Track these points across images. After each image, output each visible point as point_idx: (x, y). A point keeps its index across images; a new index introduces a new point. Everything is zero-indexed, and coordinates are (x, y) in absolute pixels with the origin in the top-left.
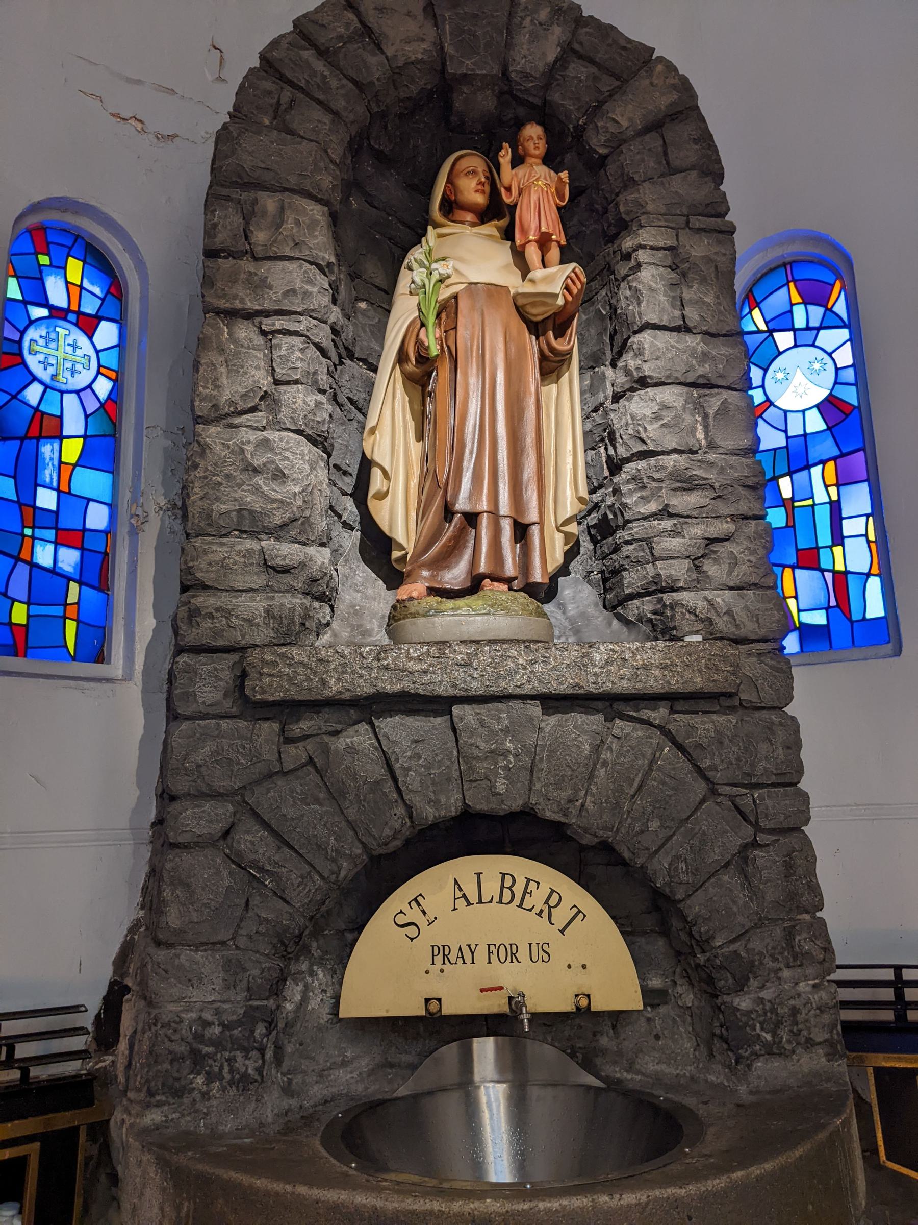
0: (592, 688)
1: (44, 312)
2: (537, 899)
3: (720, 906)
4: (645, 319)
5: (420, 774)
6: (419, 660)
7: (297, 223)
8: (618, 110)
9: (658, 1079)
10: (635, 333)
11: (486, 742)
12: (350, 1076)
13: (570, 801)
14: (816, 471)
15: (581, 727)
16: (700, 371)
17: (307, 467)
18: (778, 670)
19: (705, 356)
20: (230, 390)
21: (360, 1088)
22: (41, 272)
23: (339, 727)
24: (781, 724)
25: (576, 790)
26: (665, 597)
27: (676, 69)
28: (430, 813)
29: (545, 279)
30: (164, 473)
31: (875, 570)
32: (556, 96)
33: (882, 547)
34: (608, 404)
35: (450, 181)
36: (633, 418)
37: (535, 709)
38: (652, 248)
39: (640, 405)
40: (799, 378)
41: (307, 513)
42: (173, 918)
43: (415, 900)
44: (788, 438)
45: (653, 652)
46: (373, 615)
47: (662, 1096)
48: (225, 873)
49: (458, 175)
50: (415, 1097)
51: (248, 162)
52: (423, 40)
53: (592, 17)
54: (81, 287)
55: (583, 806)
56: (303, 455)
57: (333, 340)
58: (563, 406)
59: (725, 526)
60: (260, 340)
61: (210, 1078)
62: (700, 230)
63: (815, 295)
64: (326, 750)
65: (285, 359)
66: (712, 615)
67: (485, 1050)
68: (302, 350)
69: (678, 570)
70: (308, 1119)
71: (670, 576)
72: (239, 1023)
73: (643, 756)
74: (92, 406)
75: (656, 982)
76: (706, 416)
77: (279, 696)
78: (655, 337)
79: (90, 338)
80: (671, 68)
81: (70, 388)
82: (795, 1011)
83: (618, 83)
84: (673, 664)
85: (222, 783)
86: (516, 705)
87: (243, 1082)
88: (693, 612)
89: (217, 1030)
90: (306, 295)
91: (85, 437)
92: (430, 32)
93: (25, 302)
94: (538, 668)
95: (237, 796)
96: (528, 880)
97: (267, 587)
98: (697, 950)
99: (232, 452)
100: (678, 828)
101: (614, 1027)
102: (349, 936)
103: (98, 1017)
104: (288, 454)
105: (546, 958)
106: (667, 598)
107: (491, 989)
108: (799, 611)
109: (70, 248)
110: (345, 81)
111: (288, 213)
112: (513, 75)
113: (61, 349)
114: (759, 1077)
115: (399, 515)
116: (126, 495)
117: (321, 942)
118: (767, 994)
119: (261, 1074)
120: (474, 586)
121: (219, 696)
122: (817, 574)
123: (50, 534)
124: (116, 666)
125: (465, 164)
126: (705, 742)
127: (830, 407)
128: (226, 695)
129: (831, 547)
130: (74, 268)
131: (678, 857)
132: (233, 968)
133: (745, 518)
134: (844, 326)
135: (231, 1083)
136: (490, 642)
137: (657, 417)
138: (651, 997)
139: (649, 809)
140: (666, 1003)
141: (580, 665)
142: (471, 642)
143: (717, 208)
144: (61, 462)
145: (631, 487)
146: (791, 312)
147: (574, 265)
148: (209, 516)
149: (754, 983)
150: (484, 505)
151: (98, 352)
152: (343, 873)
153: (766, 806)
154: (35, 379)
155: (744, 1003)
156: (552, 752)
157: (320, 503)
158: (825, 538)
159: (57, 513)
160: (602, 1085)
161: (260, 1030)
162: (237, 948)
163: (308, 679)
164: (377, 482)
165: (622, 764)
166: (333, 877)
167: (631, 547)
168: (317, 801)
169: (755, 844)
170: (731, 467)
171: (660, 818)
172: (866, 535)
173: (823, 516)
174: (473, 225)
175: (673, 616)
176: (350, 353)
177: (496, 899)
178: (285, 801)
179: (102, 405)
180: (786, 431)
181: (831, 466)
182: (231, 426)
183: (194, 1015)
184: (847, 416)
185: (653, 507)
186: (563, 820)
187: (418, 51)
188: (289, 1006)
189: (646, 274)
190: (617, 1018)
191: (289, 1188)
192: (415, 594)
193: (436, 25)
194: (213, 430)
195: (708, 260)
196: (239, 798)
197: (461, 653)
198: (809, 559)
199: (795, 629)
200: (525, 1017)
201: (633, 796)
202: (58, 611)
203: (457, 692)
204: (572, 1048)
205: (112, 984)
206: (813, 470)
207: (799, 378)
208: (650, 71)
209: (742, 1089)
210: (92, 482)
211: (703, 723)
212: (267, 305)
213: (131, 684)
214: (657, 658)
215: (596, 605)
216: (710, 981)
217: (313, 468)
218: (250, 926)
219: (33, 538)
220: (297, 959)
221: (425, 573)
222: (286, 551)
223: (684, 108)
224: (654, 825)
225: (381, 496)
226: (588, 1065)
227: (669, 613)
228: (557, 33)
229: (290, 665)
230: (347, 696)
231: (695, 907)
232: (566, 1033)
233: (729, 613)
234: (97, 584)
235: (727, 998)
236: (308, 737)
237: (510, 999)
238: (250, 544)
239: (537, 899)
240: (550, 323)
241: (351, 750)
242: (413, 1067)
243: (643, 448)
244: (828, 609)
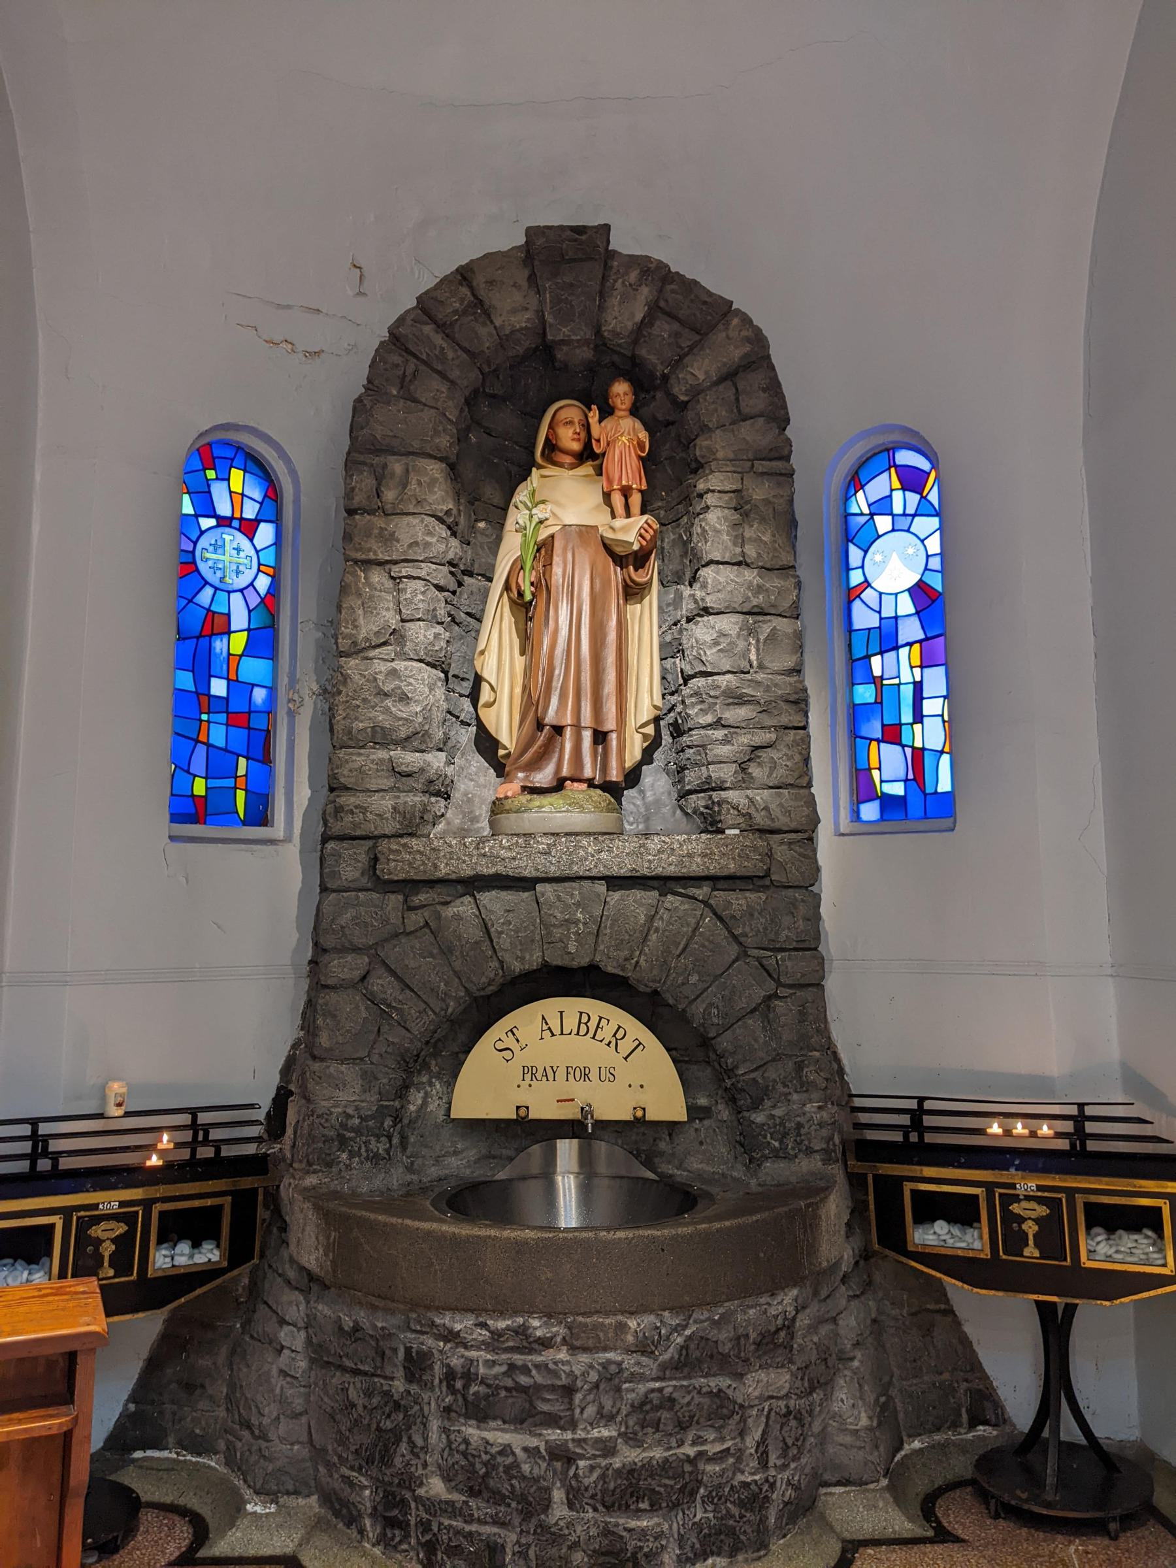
0: (646, 872)
1: (212, 522)
2: (607, 1033)
3: (745, 1042)
4: (710, 557)
5: (510, 937)
6: (509, 849)
7: (420, 483)
8: (695, 364)
9: (700, 1176)
10: (703, 566)
11: (562, 913)
12: (461, 1162)
13: (626, 959)
14: (903, 652)
15: (637, 902)
16: (755, 602)
17: (427, 689)
18: (804, 856)
19: (760, 589)
20: (367, 628)
21: (468, 1172)
22: (209, 486)
23: (449, 899)
24: (803, 901)
25: (632, 951)
26: (714, 794)
27: (751, 321)
28: (517, 967)
29: (624, 529)
30: (316, 662)
31: (947, 749)
32: (643, 352)
33: (951, 726)
34: (684, 621)
35: (551, 427)
36: (697, 642)
37: (601, 887)
38: (719, 492)
39: (702, 632)
40: (895, 561)
41: (426, 727)
42: (324, 1040)
43: (511, 1031)
44: (881, 619)
45: (698, 843)
46: (483, 802)
47: (697, 1186)
48: (363, 1008)
49: (557, 424)
50: (510, 1180)
51: (379, 431)
52: (527, 309)
53: (677, 273)
54: (243, 495)
55: (637, 962)
56: (423, 680)
57: (451, 573)
58: (645, 622)
59: (768, 735)
60: (389, 584)
61: (351, 1155)
62: (763, 474)
63: (912, 481)
64: (438, 917)
65: (409, 602)
66: (752, 811)
67: (567, 1150)
68: (423, 593)
69: (726, 772)
70: (424, 1190)
71: (720, 778)
72: (372, 1117)
73: (688, 925)
74: (254, 601)
75: (703, 1101)
76: (758, 641)
77: (402, 876)
78: (717, 573)
79: (251, 540)
80: (746, 320)
81: (236, 587)
82: (799, 1126)
83: (698, 337)
84: (712, 853)
85: (359, 941)
86: (586, 884)
87: (375, 1158)
88: (736, 808)
89: (357, 1121)
90: (427, 545)
91: (249, 630)
92: (533, 301)
93: (197, 516)
94: (603, 855)
95: (373, 952)
96: (601, 1018)
97: (393, 789)
98: (726, 1077)
99: (368, 680)
100: (714, 981)
101: (670, 1135)
102: (461, 1056)
103: (268, 1113)
104: (411, 680)
105: (612, 1078)
106: (716, 795)
107: (565, 1101)
108: (882, 781)
109: (232, 460)
110: (460, 352)
111: (412, 474)
112: (606, 334)
113: (227, 554)
114: (767, 1174)
115: (504, 723)
116: (284, 680)
117: (439, 1060)
118: (778, 1112)
119: (388, 1154)
120: (559, 785)
121: (358, 874)
122: (898, 748)
123: (222, 718)
124: (278, 829)
125: (563, 415)
126: (738, 914)
127: (920, 592)
128: (362, 874)
129: (912, 724)
130: (236, 476)
131: (711, 1005)
132: (368, 1078)
133: (786, 728)
134: (937, 515)
135: (367, 1159)
136: (567, 834)
137: (716, 643)
138: (694, 1111)
139: (691, 966)
140: (709, 1118)
141: (636, 854)
142: (553, 834)
143: (781, 453)
144: (229, 654)
145: (693, 700)
146: (890, 496)
147: (645, 517)
148: (350, 732)
149: (768, 1103)
150: (568, 719)
151: (257, 552)
152: (450, 1010)
153: (791, 963)
154: (207, 583)
155: (759, 1118)
156: (615, 921)
157: (438, 716)
158: (907, 716)
159: (227, 699)
160: (657, 1178)
161: (388, 1122)
162: (372, 1063)
163: (424, 864)
164: (485, 695)
165: (670, 931)
166: (443, 1013)
167: (691, 751)
168: (432, 955)
169: (775, 996)
170: (776, 685)
171: (699, 973)
172: (942, 716)
173: (907, 692)
174: (573, 467)
175: (719, 812)
176: (468, 572)
177: (575, 1031)
178: (409, 955)
179: (263, 600)
180: (880, 612)
181: (917, 646)
182: (367, 658)
183: (340, 1110)
184: (933, 601)
185: (709, 719)
186: (621, 973)
187: (522, 320)
188: (412, 1108)
189: (713, 517)
190: (672, 1127)
191: (400, 1221)
192: (509, 794)
193: (538, 292)
194: (353, 662)
195: (767, 502)
196: (373, 951)
197: (543, 843)
198: (892, 734)
199: (877, 798)
200: (589, 1122)
201: (679, 956)
202: (230, 782)
203: (539, 874)
204: (637, 1150)
205: (279, 1089)
206: (901, 650)
207: (895, 561)
208: (728, 324)
209: (753, 1182)
210: (254, 669)
211: (737, 899)
212: (394, 557)
213: (290, 846)
214: (699, 848)
215: (669, 794)
216: (733, 1100)
217: (431, 689)
218: (381, 1048)
219: (208, 722)
220: (419, 1072)
221: (520, 775)
222: (409, 759)
223: (757, 356)
224: (694, 979)
225: (489, 705)
226: (648, 1164)
227: (716, 809)
228: (645, 293)
229: (410, 853)
230: (453, 876)
231: (724, 1043)
232: (633, 1138)
233: (766, 808)
234: (260, 757)
235: (746, 1114)
236: (425, 906)
237: (582, 1109)
238: (382, 754)
239: (607, 1033)
240: (631, 559)
241: (458, 917)
242: (511, 1159)
243: (703, 669)
244: (906, 781)
